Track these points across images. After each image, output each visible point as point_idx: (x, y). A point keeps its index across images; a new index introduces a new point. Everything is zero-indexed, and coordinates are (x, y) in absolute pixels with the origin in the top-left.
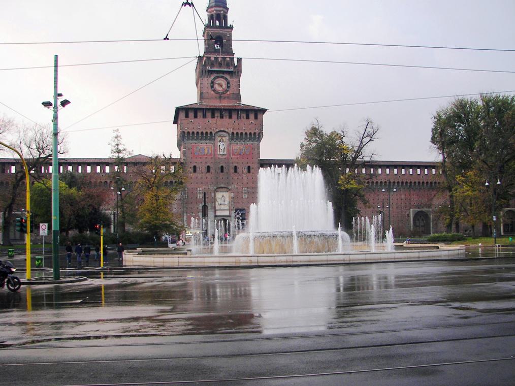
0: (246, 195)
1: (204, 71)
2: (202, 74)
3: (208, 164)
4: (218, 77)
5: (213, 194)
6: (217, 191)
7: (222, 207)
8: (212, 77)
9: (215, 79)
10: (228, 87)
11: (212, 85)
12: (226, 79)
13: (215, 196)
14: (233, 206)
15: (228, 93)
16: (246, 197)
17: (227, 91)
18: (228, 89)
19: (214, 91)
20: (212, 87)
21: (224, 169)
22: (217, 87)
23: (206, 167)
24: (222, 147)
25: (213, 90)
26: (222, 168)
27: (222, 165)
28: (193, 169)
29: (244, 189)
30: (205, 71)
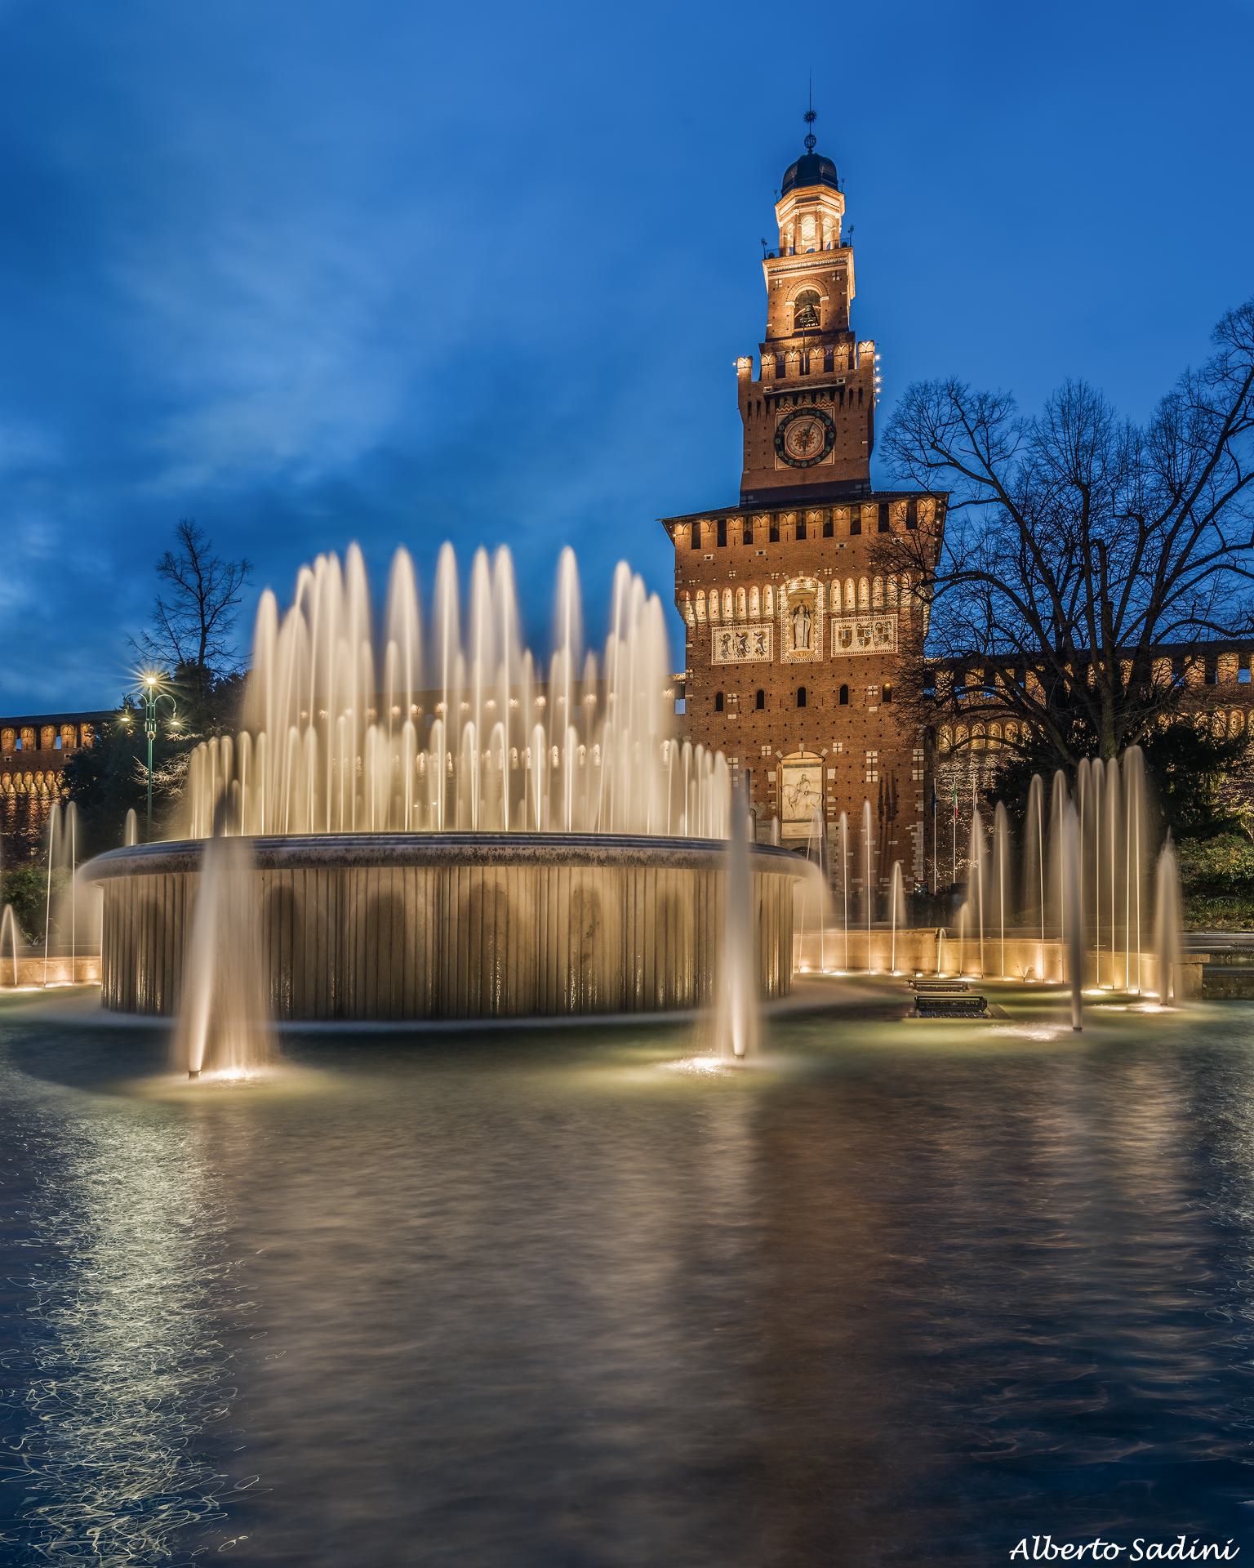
0: (875, 773)
1: (754, 408)
2: (750, 414)
3: (762, 686)
4: (796, 414)
5: (772, 776)
6: (786, 766)
7: (800, 813)
8: (780, 417)
9: (785, 423)
10: (830, 442)
11: (778, 441)
12: (823, 417)
13: (780, 777)
14: (833, 808)
15: (830, 460)
16: (875, 779)
17: (823, 456)
18: (828, 449)
19: (786, 459)
20: (780, 447)
21: (808, 697)
22: (794, 448)
23: (753, 693)
24: (800, 631)
25: (781, 458)
26: (802, 697)
27: (799, 683)
28: (713, 701)
29: (869, 754)
30: (759, 403)
